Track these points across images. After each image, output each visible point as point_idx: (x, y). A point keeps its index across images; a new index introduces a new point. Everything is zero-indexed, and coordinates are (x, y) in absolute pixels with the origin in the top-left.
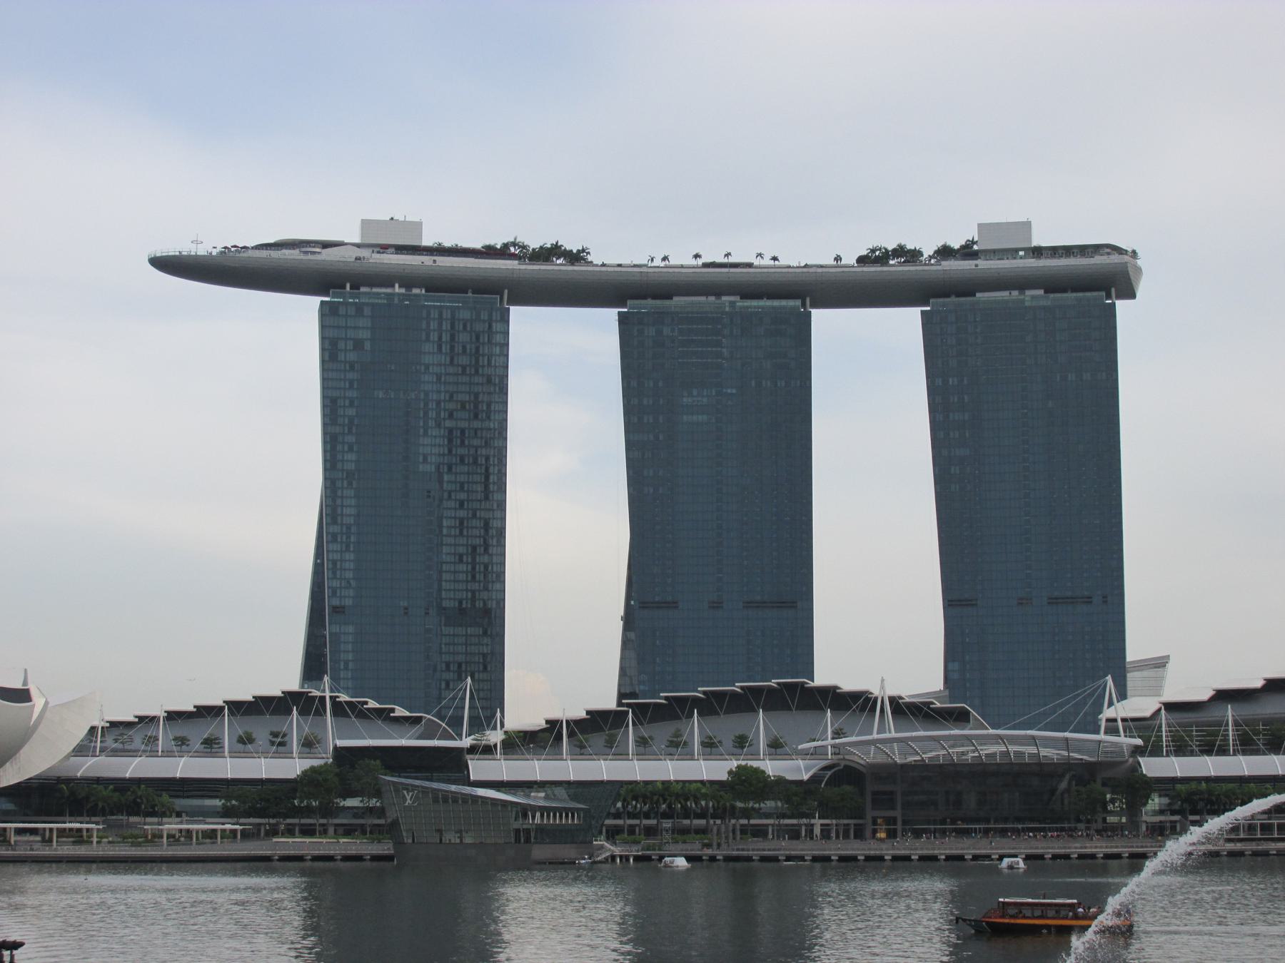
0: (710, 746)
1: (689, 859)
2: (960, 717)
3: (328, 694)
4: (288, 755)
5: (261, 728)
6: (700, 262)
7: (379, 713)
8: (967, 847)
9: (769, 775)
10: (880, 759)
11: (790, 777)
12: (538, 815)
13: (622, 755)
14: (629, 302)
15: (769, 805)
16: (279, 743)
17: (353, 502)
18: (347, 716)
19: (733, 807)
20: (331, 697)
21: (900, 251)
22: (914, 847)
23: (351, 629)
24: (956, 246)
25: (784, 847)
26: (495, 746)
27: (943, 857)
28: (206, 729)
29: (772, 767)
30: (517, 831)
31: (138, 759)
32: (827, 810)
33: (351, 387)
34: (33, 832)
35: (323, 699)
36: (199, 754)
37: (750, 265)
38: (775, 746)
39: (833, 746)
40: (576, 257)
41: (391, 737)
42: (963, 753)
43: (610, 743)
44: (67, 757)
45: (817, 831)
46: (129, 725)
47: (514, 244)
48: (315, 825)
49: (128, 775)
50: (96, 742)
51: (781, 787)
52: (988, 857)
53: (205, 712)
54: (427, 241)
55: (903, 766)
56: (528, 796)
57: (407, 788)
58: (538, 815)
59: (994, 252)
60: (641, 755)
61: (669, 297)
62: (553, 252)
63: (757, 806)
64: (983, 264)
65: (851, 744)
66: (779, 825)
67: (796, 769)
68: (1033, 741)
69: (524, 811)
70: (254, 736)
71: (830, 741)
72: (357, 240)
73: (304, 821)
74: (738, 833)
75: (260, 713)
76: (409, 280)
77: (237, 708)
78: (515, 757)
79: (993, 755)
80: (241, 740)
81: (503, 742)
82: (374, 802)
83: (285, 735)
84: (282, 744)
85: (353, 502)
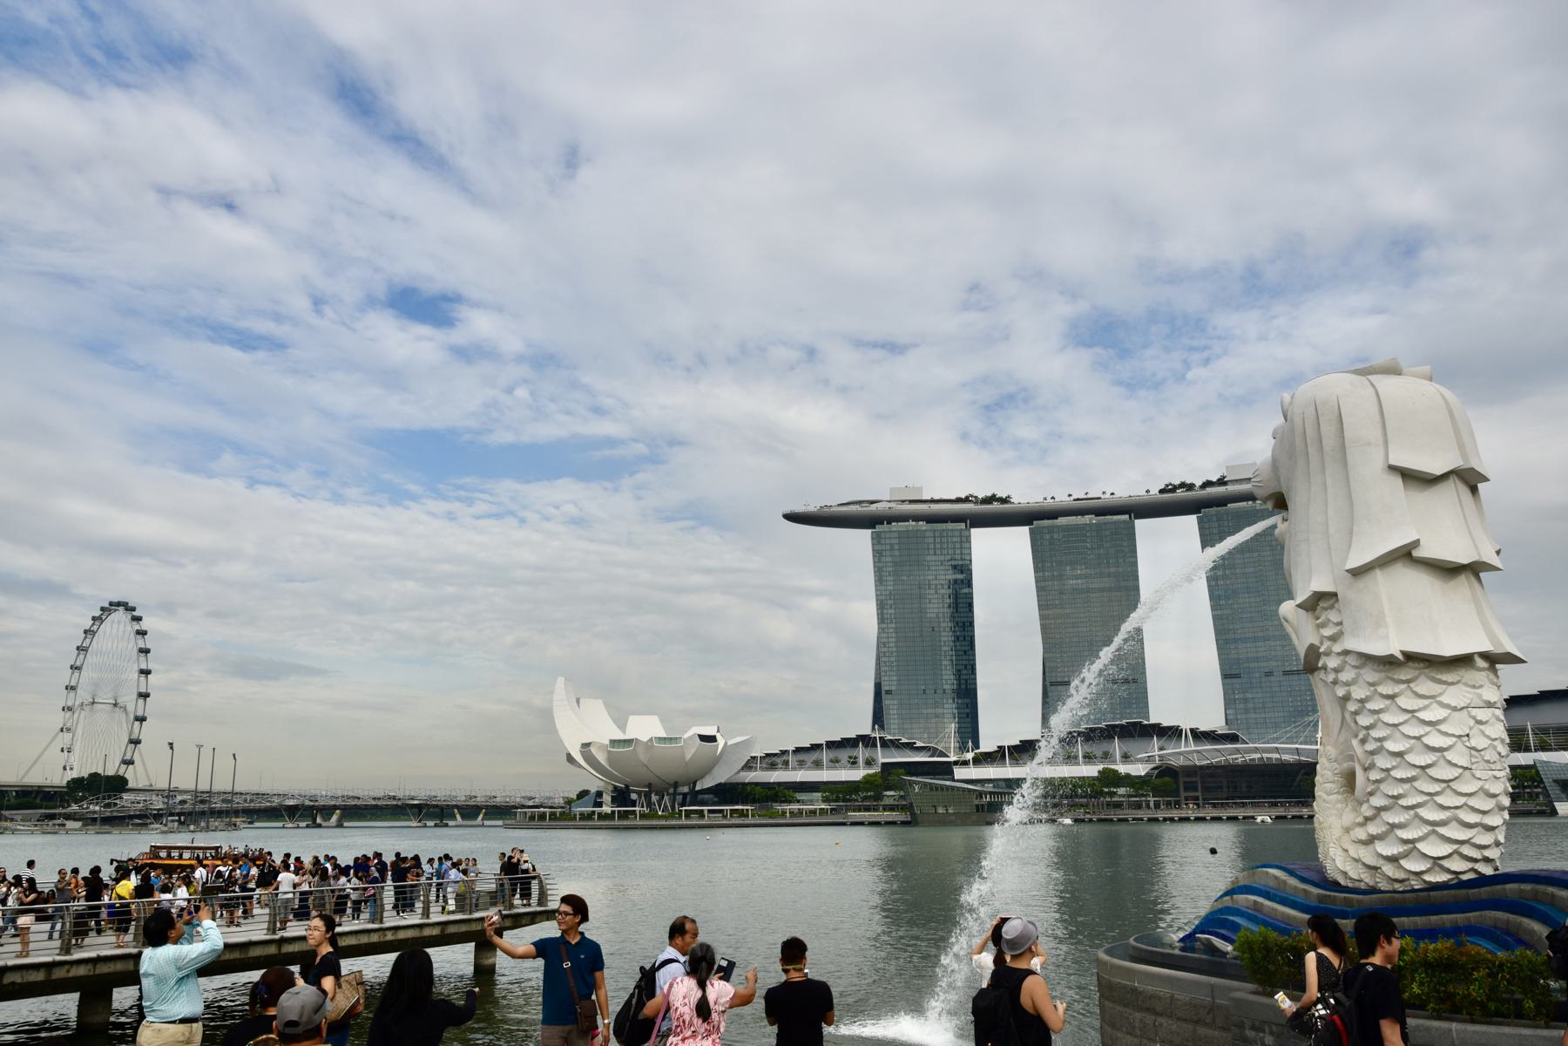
0: (1089, 758)
1: (1076, 821)
2: (1233, 738)
3: (878, 736)
4: (858, 768)
5: (844, 755)
6: (1072, 498)
7: (908, 744)
8: (1240, 813)
10: (1188, 763)
12: (988, 796)
14: (1035, 522)
15: (1122, 791)
16: (853, 762)
17: (894, 635)
18: (889, 747)
21: (1183, 485)
22: (1209, 812)
23: (895, 702)
24: (1215, 480)
25: (1131, 814)
27: (1225, 818)
28: (814, 756)
29: (1123, 769)
30: (977, 806)
32: (1157, 792)
33: (890, 575)
34: (721, 811)
36: (809, 768)
37: (1099, 498)
38: (1126, 758)
39: (1159, 756)
41: (909, 757)
42: (1236, 759)
45: (1152, 804)
46: (776, 755)
47: (972, 496)
49: (772, 781)
50: (757, 763)
51: (1128, 780)
52: (1253, 818)
54: (924, 498)
55: (1201, 767)
56: (983, 786)
57: (915, 782)
58: (988, 796)
59: (1236, 481)
61: (1057, 519)
62: (991, 499)
63: (1115, 790)
64: (1231, 488)
65: (1169, 754)
67: (1139, 770)
68: (1277, 750)
69: (980, 794)
70: (840, 757)
71: (1157, 753)
72: (889, 499)
73: (865, 803)
74: (1105, 806)
75: (844, 746)
76: (917, 518)
77: (831, 745)
79: (1254, 759)
80: (832, 761)
82: (902, 793)
83: (856, 758)
84: (854, 763)
85: (894, 635)
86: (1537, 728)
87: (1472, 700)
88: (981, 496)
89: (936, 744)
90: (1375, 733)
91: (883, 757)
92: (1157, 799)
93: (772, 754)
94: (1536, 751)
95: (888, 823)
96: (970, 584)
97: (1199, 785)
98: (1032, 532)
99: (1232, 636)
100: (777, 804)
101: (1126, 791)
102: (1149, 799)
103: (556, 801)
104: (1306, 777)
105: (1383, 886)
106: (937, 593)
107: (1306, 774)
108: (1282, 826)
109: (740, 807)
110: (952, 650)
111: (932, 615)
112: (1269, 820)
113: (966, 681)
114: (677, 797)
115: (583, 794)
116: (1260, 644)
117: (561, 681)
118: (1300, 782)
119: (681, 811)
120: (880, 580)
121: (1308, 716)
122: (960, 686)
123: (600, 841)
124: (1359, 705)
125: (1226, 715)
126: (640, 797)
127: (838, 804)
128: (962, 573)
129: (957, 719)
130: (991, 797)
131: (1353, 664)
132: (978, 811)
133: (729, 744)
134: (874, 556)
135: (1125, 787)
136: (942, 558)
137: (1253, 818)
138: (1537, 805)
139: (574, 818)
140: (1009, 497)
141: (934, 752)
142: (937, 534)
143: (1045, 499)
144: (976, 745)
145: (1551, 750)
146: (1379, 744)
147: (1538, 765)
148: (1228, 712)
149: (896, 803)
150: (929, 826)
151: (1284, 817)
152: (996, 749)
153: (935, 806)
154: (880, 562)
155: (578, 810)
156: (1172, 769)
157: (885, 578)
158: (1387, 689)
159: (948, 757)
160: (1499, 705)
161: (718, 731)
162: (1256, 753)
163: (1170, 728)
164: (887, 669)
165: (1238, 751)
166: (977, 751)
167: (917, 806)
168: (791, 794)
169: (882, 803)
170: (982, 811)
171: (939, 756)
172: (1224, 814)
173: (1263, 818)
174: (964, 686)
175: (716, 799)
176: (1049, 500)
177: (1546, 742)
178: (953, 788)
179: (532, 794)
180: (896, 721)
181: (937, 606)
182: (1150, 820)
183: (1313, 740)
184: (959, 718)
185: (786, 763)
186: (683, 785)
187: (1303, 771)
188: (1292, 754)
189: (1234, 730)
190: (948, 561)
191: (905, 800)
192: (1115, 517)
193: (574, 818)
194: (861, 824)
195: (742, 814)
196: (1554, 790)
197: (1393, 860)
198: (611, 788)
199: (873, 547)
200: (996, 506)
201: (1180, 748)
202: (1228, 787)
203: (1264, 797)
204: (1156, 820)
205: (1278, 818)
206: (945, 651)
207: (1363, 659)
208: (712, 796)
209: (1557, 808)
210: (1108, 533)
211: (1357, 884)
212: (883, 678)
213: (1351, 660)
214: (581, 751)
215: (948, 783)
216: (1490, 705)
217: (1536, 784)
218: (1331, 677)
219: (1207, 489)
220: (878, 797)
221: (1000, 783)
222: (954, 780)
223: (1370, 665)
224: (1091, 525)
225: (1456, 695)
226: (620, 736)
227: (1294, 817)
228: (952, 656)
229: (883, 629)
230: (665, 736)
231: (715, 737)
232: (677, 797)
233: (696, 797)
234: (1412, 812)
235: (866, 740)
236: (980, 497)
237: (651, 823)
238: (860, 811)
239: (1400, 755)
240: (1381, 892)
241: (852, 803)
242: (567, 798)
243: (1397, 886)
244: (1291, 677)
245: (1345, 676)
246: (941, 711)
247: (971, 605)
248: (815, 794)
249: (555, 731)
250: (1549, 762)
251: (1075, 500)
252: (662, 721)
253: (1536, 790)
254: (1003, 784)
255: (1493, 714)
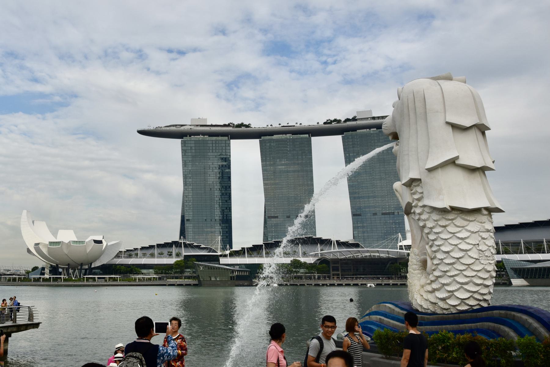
3: (182, 242)
4: (172, 257)
5: (165, 251)
8: (359, 282)
9: (302, 262)
11: (308, 262)
13: (262, 256)
16: (170, 255)
19: (292, 270)
20: (183, 242)
22: (344, 282)
26: (227, 254)
27: (352, 284)
28: (151, 251)
31: (132, 259)
35: (181, 243)
36: (148, 257)
39: (321, 254)
40: (248, 126)
43: (258, 254)
44: (113, 259)
45: (316, 277)
46: (131, 250)
48: (178, 276)
52: (366, 284)
53: (151, 247)
60: (267, 257)
63: (299, 270)
66: (305, 276)
67: (310, 260)
70: (163, 253)
71: (319, 252)
73: (175, 275)
77: (159, 246)
78: (233, 257)
80: (159, 254)
81: (229, 254)
82: (194, 270)
83: (171, 252)
84: (170, 255)
86: (504, 243)
87: (480, 228)
88: (236, 123)
89: (211, 246)
91: (185, 252)
92: (319, 275)
93: (129, 250)
94: (503, 254)
95: (187, 285)
96: (229, 167)
97: (340, 268)
98: (261, 143)
99: (358, 195)
100: (132, 275)
101: (304, 271)
102: (315, 275)
103: (21, 272)
104: (391, 265)
106: (213, 171)
107: (392, 263)
108: (380, 289)
109: (113, 276)
110: (220, 200)
111: (210, 182)
112: (374, 286)
113: (227, 215)
114: (82, 271)
115: (35, 269)
116: (371, 199)
117: (25, 212)
118: (388, 267)
119: (84, 277)
120: (185, 164)
121: (394, 235)
122: (223, 218)
123: (44, 291)
125: (353, 234)
126: (63, 270)
127: (162, 275)
128: (226, 162)
129: (221, 234)
130: (238, 273)
132: (231, 279)
133: (108, 245)
134: (182, 153)
135: (304, 269)
136: (216, 154)
137: (366, 284)
138: (503, 280)
139: (30, 280)
140: (250, 124)
141: (210, 250)
142: (214, 142)
143: (268, 126)
144: (231, 247)
145: (510, 253)
147: (503, 261)
148: (354, 233)
149: (191, 275)
150: (207, 287)
151: (381, 285)
152: (241, 249)
153: (210, 277)
154: (185, 155)
155: (32, 276)
156: (326, 260)
157: (187, 164)
159: (217, 253)
160: (492, 231)
161: (103, 238)
162: (368, 253)
163: (326, 240)
164: (187, 208)
165: (359, 252)
166: (231, 250)
167: (201, 277)
168: (139, 270)
169: (184, 275)
170: (234, 280)
171: (212, 252)
172: (352, 283)
173: (371, 284)
174: (225, 218)
175: (101, 272)
176: (269, 126)
177: (507, 249)
178: (219, 268)
179: (9, 268)
180: (192, 235)
181: (213, 178)
182: (316, 285)
183: (395, 247)
184: (222, 233)
185: (137, 255)
186: (85, 265)
187: (390, 262)
188: (385, 254)
189: (357, 241)
190: (219, 155)
191: (195, 274)
192: (302, 136)
193: (30, 280)
194: (173, 285)
195: (115, 280)
196: (511, 273)
198: (49, 266)
199: (182, 148)
200: (243, 129)
201: (331, 250)
202: (354, 269)
203: (371, 275)
204: (318, 285)
205: (377, 285)
206: (216, 201)
208: (99, 270)
209: (512, 281)
210: (298, 143)
212: (185, 213)
214: (34, 247)
215: (217, 265)
216: (488, 231)
217: (502, 270)
219: (347, 123)
220: (182, 272)
221: (242, 266)
222: (219, 264)
224: (290, 139)
225: (474, 226)
226: (54, 240)
227: (385, 284)
228: (220, 202)
229: (186, 189)
230: (76, 240)
231: (102, 241)
232: (82, 271)
233: (92, 271)
235: (176, 244)
236: (235, 124)
237: (69, 283)
238: (173, 279)
241: (169, 275)
242: (27, 270)
244: (386, 216)
246: (213, 230)
247: (229, 178)
248: (151, 270)
249: (22, 237)
250: (509, 259)
251: (282, 127)
252: (75, 233)
253: (502, 273)
254: (244, 266)
255: (489, 235)
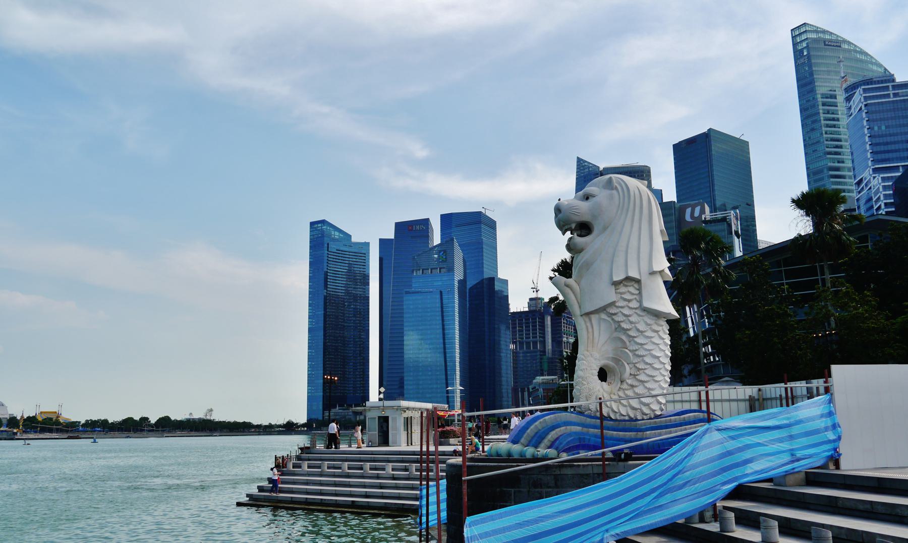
90: (645, 347)
105: (639, 418)
124: (640, 333)
131: (641, 314)
146: (648, 352)
158: (656, 327)
197: (647, 405)
207: (646, 313)
211: (622, 418)
213: (638, 311)
218: (619, 318)
223: (649, 316)
234: (658, 383)
239: (658, 358)
240: (637, 420)
243: (645, 417)
245: (631, 319)
